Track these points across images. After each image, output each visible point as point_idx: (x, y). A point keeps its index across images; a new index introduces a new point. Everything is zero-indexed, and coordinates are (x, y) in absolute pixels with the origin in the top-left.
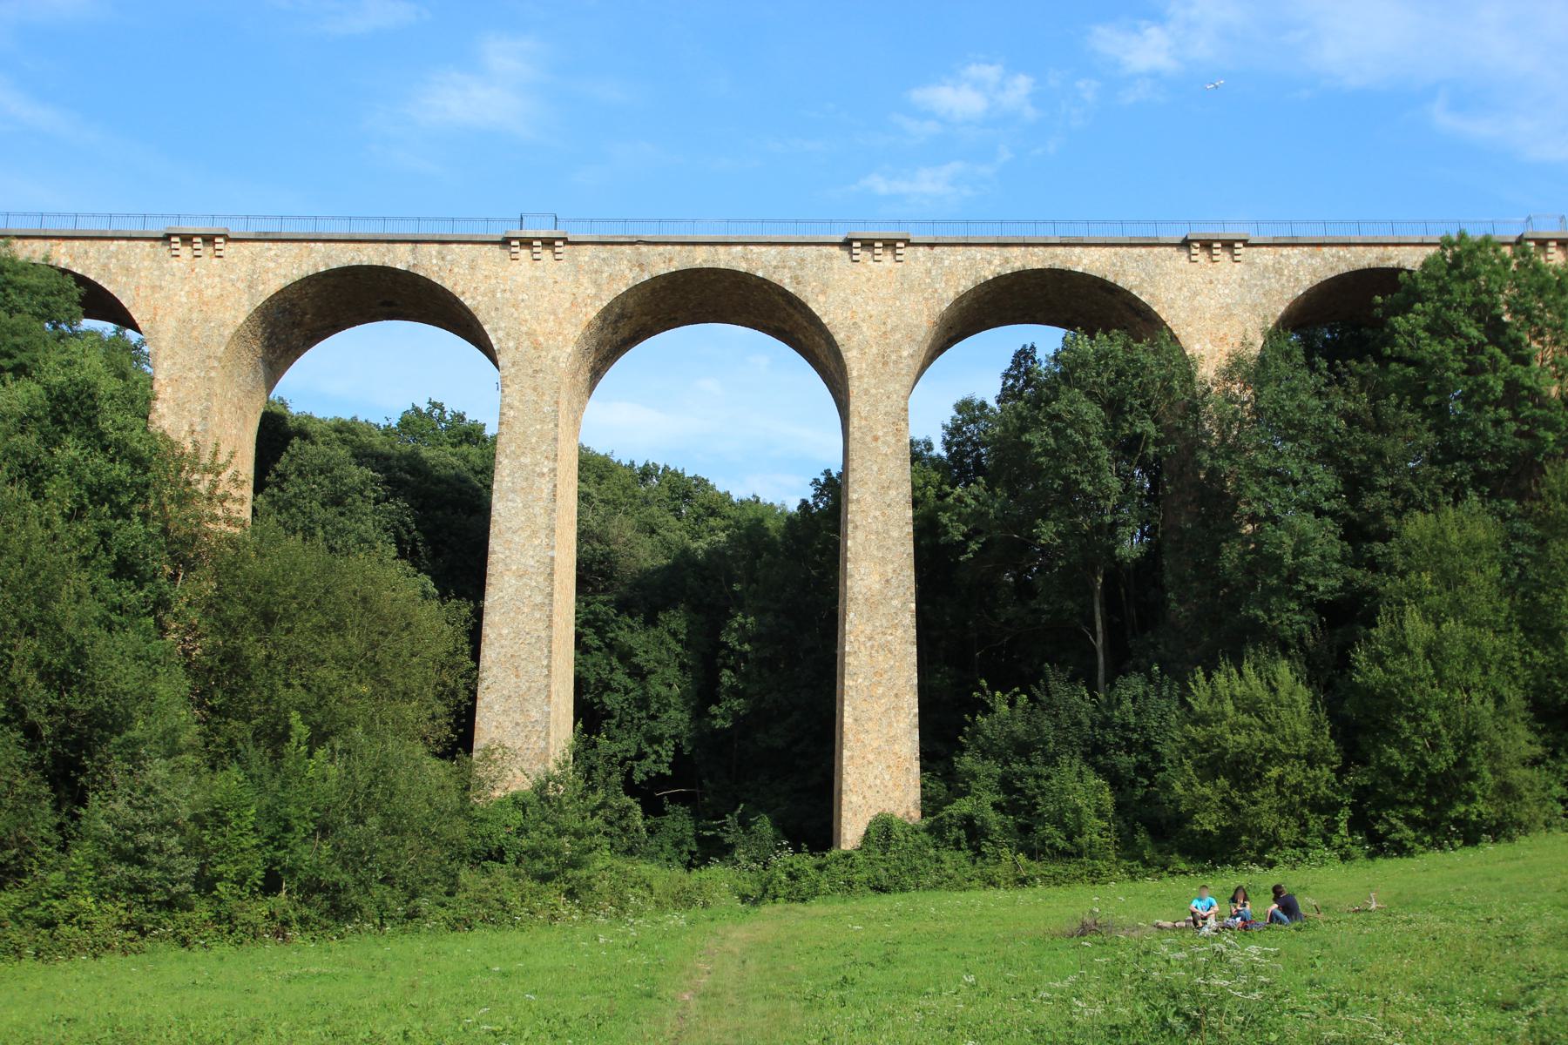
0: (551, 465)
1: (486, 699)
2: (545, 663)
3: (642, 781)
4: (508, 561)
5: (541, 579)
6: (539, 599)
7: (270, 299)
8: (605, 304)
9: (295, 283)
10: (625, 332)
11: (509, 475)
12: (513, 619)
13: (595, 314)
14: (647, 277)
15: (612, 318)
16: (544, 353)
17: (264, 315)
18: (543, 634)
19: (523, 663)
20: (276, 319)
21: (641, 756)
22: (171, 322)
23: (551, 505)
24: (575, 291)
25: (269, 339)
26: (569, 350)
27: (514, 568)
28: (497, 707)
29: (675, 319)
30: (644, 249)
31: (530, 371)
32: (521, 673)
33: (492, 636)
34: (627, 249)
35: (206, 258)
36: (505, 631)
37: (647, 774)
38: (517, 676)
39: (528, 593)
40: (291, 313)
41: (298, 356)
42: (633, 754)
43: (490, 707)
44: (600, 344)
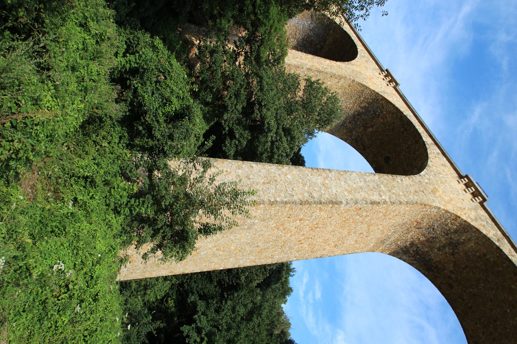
0: (388, 200)
1: (244, 166)
2: (278, 199)
3: (183, 332)
4: (329, 179)
5: (327, 196)
6: (315, 195)
7: (384, 99)
8: (472, 223)
9: (394, 106)
10: (435, 255)
11: (371, 179)
12: (297, 181)
13: (465, 219)
14: (497, 244)
15: (455, 237)
16: (433, 196)
17: (373, 100)
18: (295, 198)
19: (273, 186)
20: (370, 111)
21: (199, 331)
22: (358, 69)
23: (368, 201)
24: (466, 209)
25: (359, 114)
26: (442, 207)
27: (327, 181)
28: (240, 171)
29: (451, 286)
30: (506, 241)
31: (422, 189)
32: (267, 186)
33: (284, 170)
34: (499, 233)
35: (384, 82)
36: (289, 176)
37: (188, 336)
38: (264, 183)
39: (316, 189)
40: (373, 118)
41: (345, 140)
42: (199, 324)
43: (239, 168)
44: (430, 241)
